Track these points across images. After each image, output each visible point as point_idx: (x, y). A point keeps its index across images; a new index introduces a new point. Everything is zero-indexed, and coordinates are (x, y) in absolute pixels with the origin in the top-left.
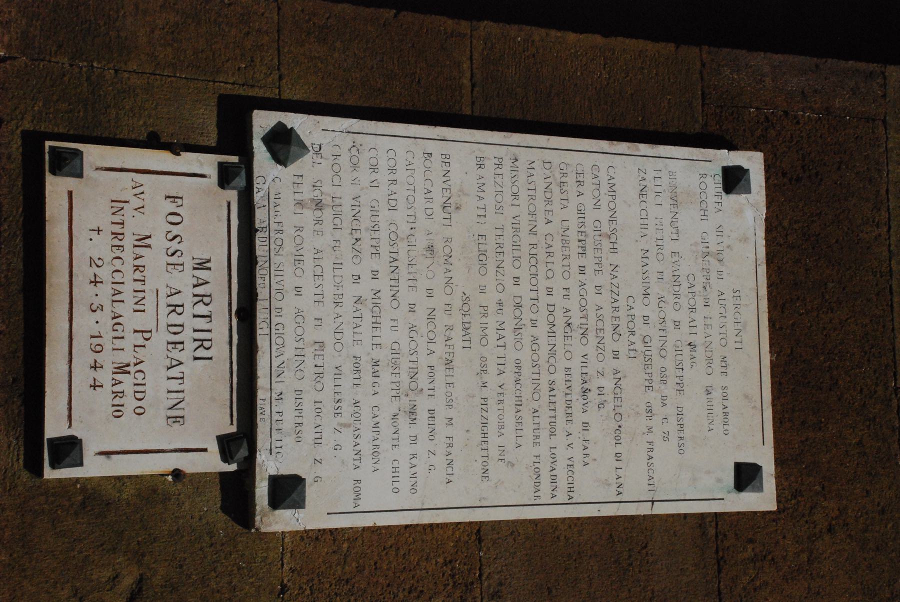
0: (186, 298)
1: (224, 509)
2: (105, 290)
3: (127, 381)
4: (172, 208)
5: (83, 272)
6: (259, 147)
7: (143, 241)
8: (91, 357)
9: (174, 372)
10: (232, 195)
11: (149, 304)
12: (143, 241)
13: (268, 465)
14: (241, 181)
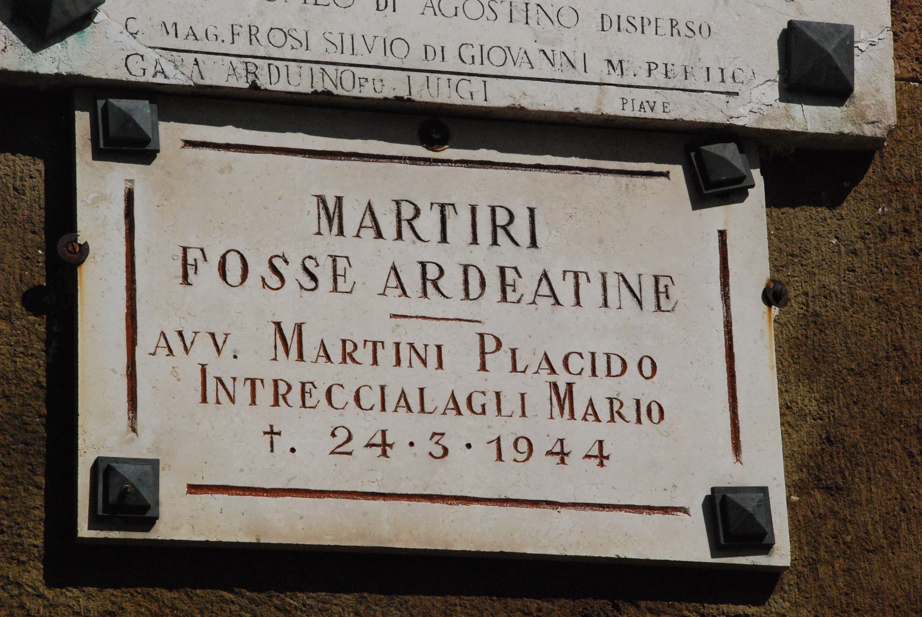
0: (407, 256)
1: (834, 202)
2: (401, 426)
4: (208, 272)
5: (363, 470)
7: (290, 340)
8: (541, 462)
9: (565, 290)
10: (170, 134)
11: (425, 335)
13: (758, 103)
14: (141, 110)
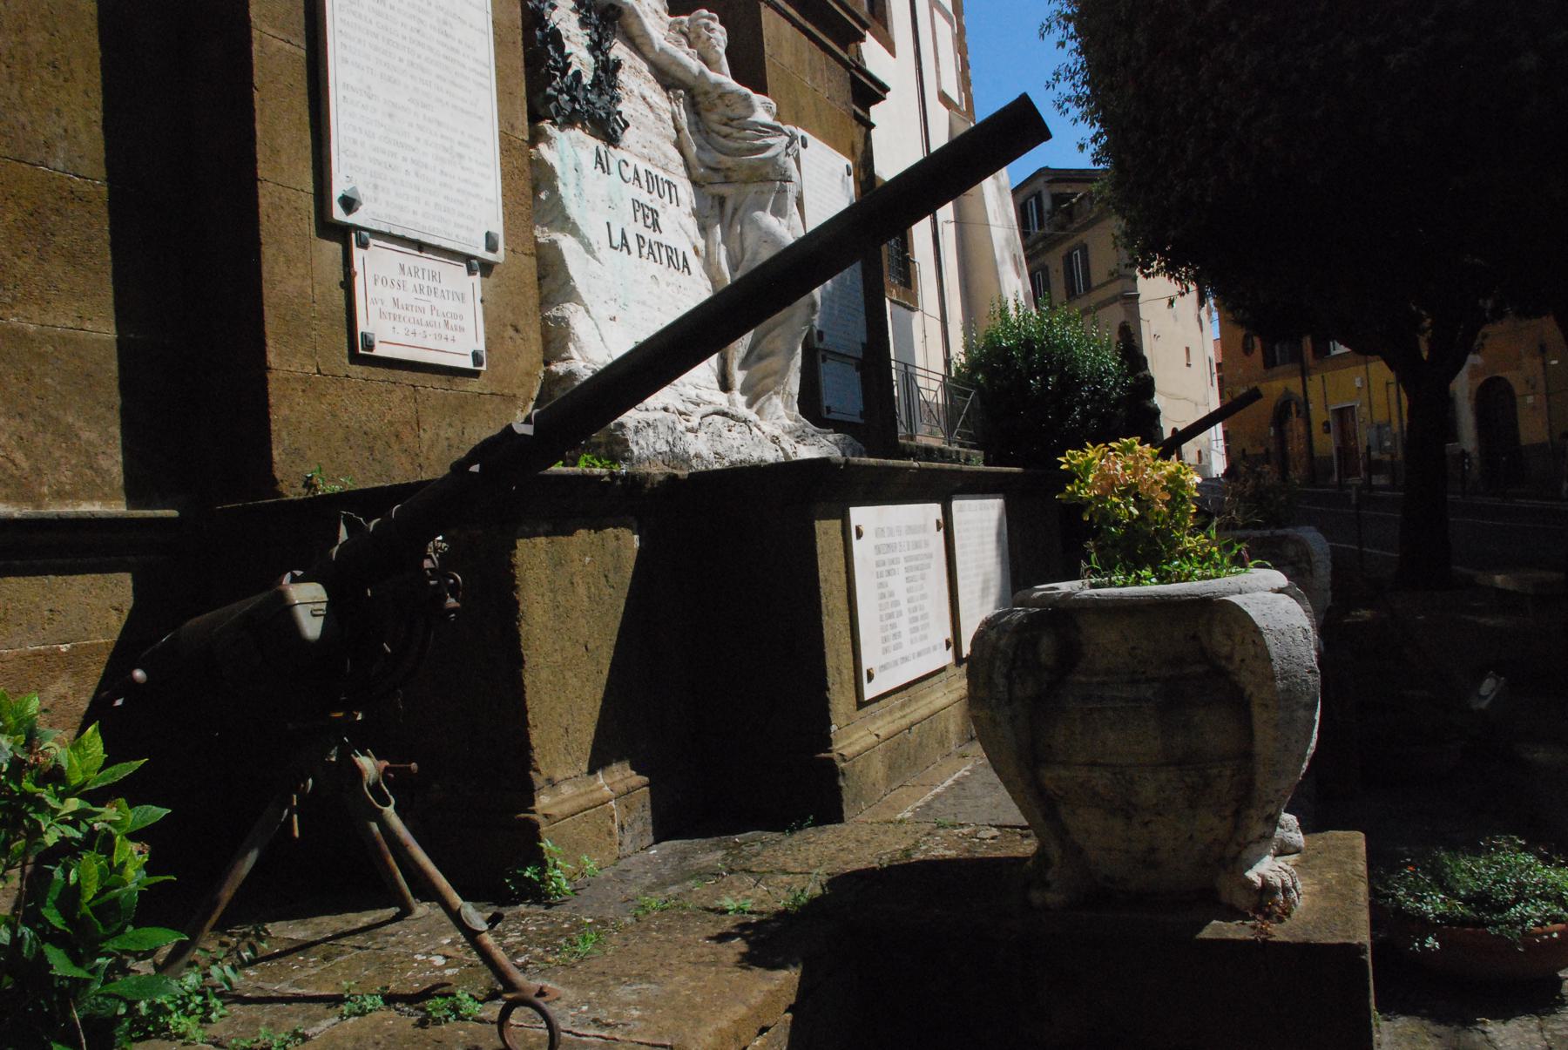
2: (419, 329)
3: (452, 322)
5: (411, 340)
6: (351, 219)
10: (372, 242)
11: (421, 304)
12: (396, 302)
13: (481, 251)
14: (366, 234)
